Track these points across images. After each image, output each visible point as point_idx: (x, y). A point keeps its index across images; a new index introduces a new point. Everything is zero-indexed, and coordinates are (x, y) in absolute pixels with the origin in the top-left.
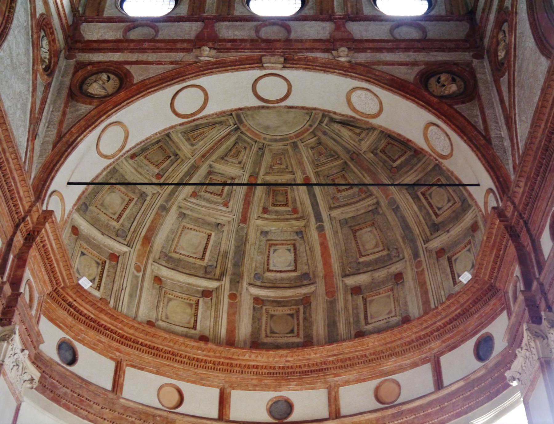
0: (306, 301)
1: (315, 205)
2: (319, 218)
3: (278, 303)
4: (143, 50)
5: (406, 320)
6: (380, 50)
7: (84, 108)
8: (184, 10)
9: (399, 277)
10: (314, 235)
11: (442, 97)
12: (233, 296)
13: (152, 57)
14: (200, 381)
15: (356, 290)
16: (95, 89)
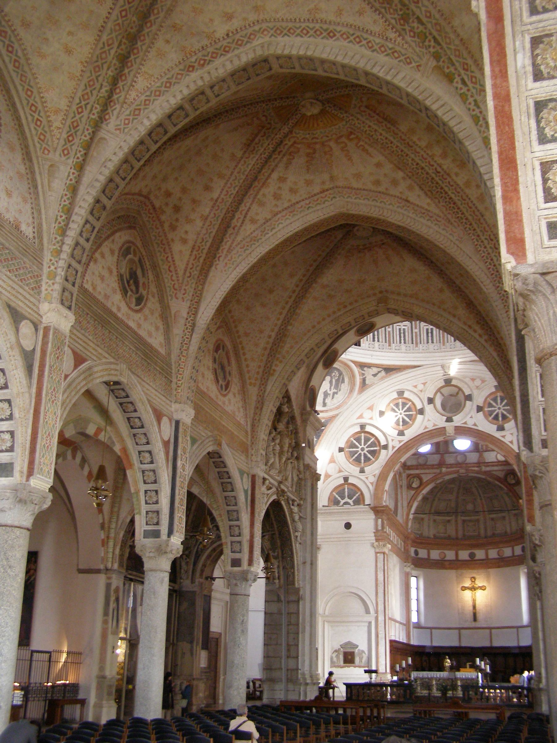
0: (478, 521)
1: (479, 493)
2: (480, 496)
3: (470, 521)
4: (425, 469)
5: (506, 532)
6: (493, 466)
7: (413, 492)
8: (434, 450)
9: (504, 518)
10: (479, 500)
11: (510, 484)
12: (456, 521)
13: (427, 471)
14: (450, 549)
15: (492, 519)
16: (414, 485)
